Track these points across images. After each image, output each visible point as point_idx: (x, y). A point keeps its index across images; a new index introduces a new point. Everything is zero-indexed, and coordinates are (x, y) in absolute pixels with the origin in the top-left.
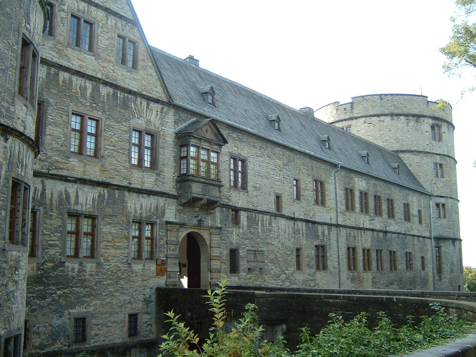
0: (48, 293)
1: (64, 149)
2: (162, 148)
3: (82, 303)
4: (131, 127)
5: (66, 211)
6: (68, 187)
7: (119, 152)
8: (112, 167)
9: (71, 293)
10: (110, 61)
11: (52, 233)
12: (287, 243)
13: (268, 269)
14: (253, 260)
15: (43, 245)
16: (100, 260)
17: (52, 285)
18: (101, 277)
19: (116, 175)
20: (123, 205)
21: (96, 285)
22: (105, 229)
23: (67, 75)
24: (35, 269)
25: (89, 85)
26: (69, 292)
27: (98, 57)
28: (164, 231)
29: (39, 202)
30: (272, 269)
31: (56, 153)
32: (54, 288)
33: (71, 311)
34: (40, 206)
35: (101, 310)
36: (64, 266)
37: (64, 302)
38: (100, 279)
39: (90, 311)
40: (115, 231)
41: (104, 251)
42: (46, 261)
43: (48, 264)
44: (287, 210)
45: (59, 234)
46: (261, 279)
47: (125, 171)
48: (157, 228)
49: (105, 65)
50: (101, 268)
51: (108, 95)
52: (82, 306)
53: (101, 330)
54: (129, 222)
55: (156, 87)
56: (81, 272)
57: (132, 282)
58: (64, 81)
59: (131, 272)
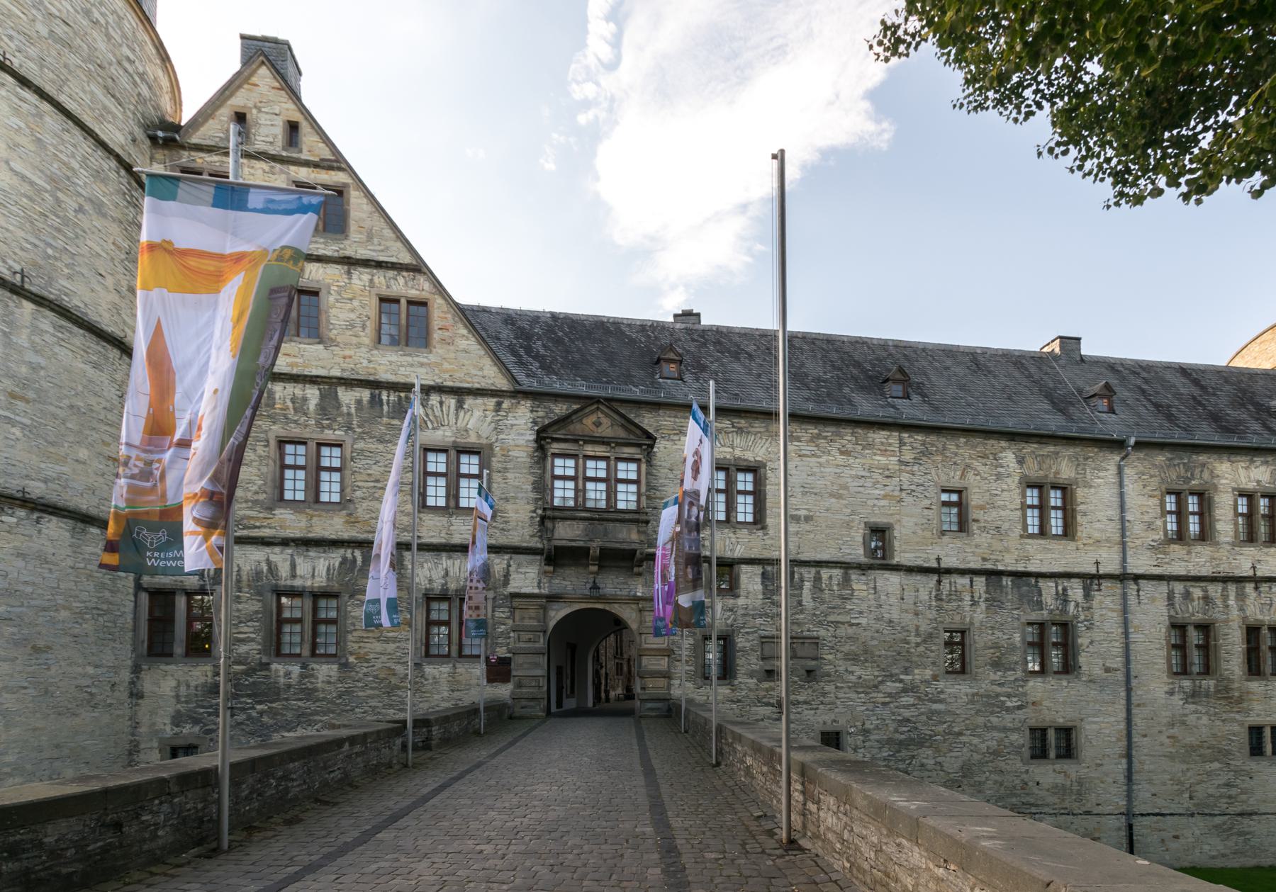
3: (310, 723)
9: (286, 708)
12: (908, 619)
21: (340, 697)
25: (313, 394)
41: (356, 646)
44: (907, 555)
49: (347, 353)
51: (359, 402)
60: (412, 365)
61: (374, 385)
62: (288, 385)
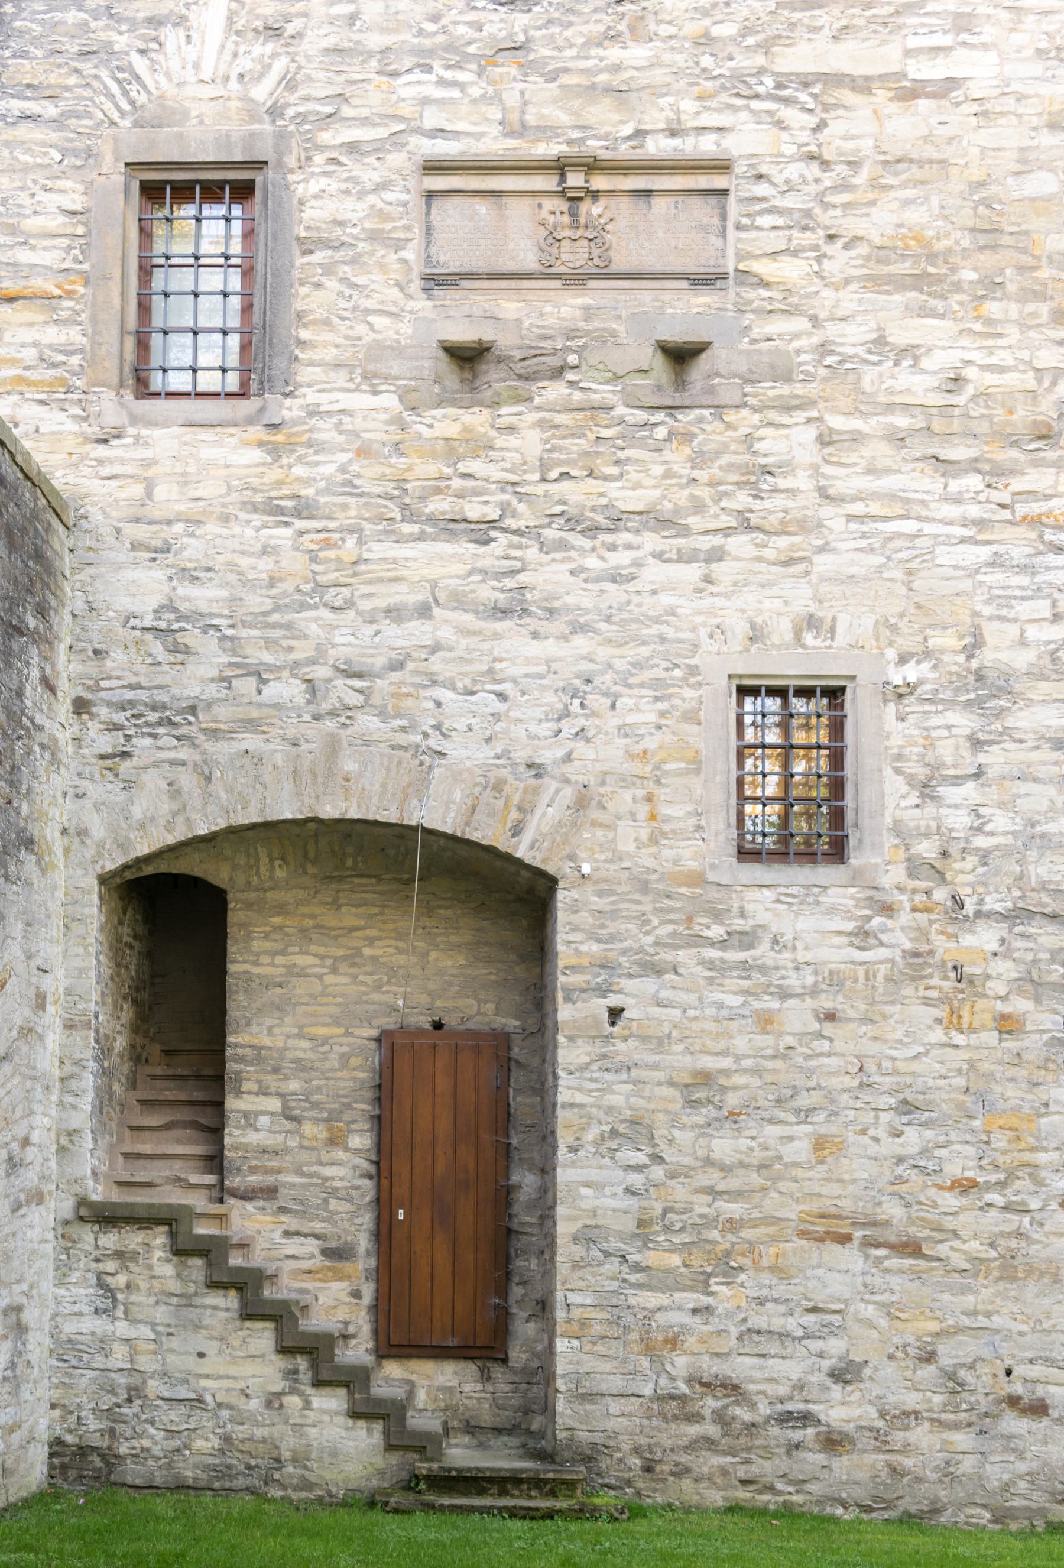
13: (824, 348)
14: (530, 261)
30: (910, 353)
46: (677, 457)
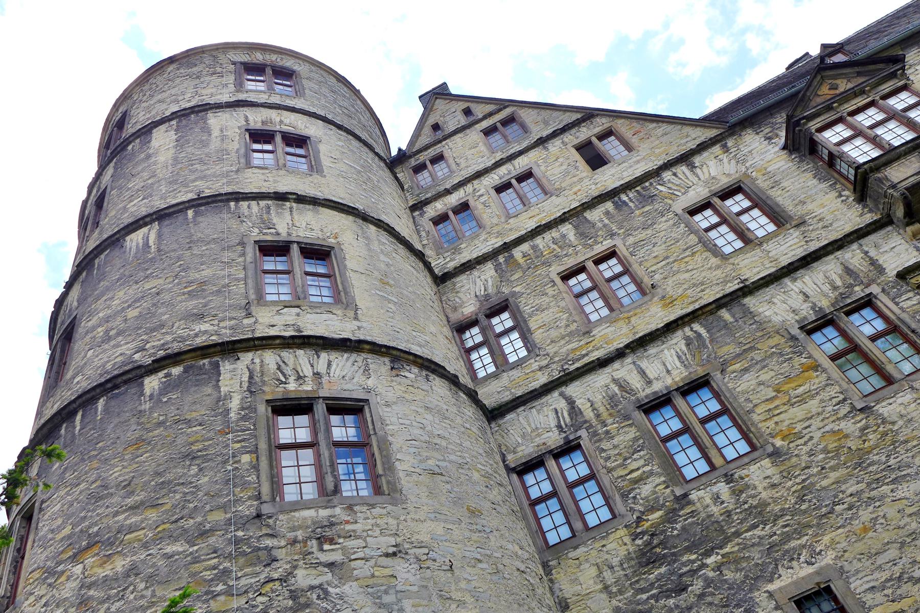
0: (685, 573)
1: (573, 327)
2: (773, 187)
3: (793, 556)
4: (680, 212)
5: (632, 407)
6: (613, 371)
7: (683, 258)
8: (685, 286)
10: (581, 180)
11: (625, 459)
15: (619, 489)
16: (773, 445)
17: (685, 553)
18: (804, 477)
19: (703, 291)
20: (756, 321)
21: (801, 499)
22: (743, 385)
23: (525, 247)
24: (627, 540)
25: (567, 229)
26: (736, 548)
27: (558, 192)
28: (911, 294)
29: (572, 425)
31: (563, 342)
32: (694, 557)
33: (771, 587)
34: (577, 431)
35: (860, 547)
36: (690, 503)
37: (739, 576)
38: (804, 481)
39: (828, 565)
40: (772, 373)
41: (771, 424)
42: (643, 513)
43: (650, 517)
45: (642, 453)
47: (719, 272)
48: (884, 301)
49: (575, 189)
50: (789, 459)
51: (607, 213)
52: (795, 563)
53: (901, 598)
54: (793, 338)
55: (687, 136)
56: (741, 492)
57: (906, 442)
58: (524, 256)
59: (883, 423)
60: (631, 167)
61: (611, 195)
62: (544, 235)
